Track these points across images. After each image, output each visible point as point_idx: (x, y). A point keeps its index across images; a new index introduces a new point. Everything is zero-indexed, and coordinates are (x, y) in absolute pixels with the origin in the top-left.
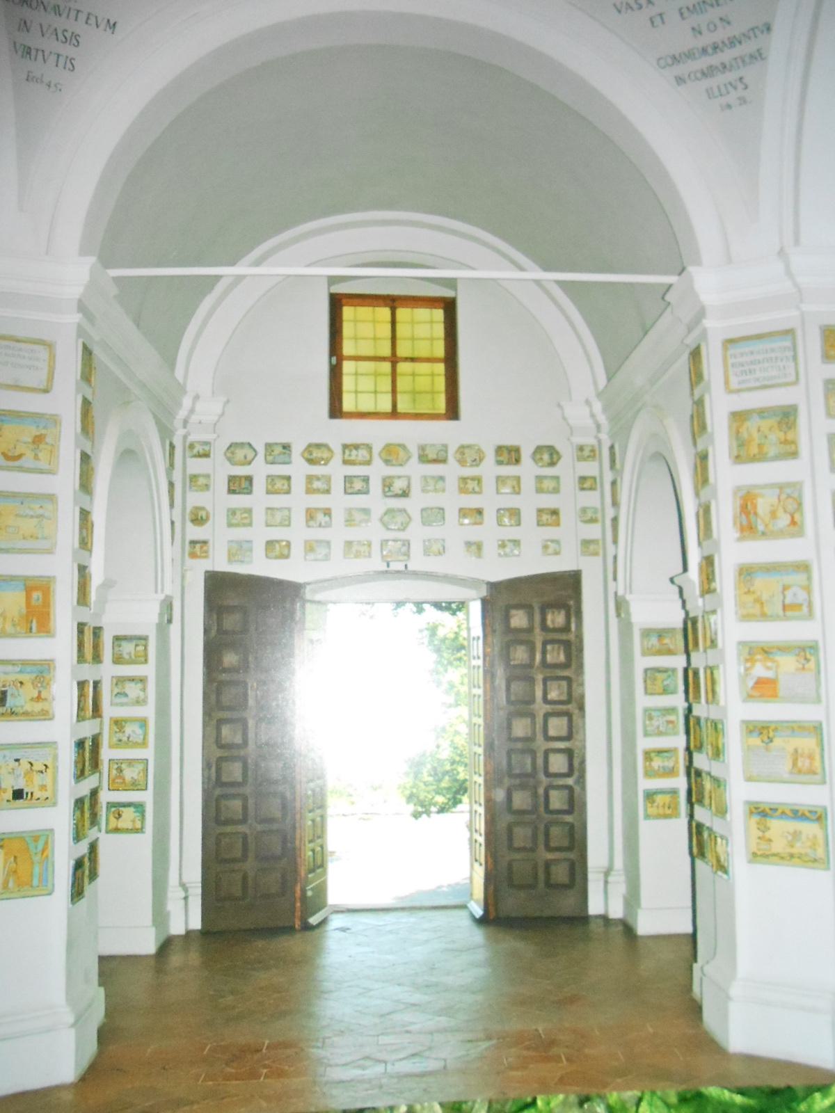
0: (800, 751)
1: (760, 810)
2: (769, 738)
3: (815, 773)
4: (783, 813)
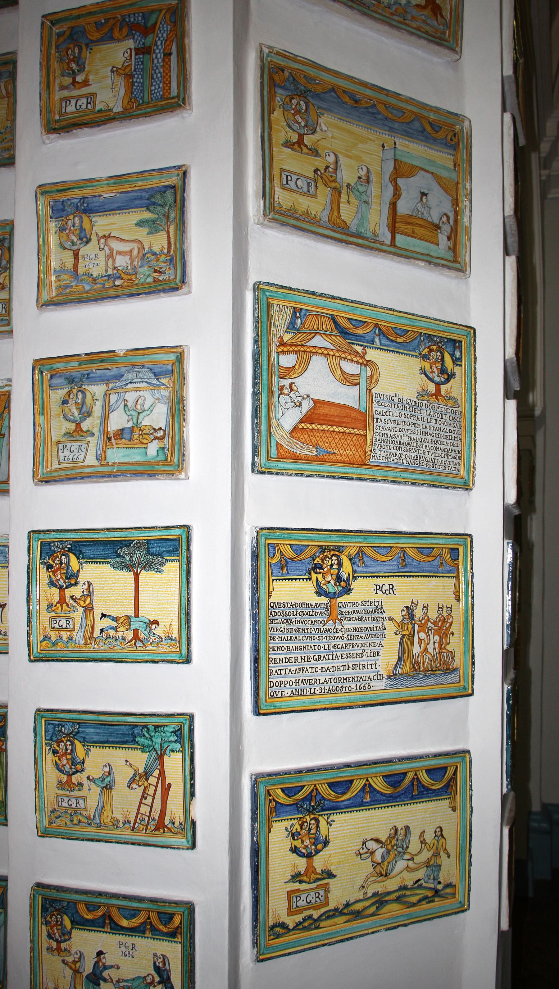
0: (419, 613)
1: (301, 795)
2: (339, 579)
3: (449, 670)
4: (368, 788)
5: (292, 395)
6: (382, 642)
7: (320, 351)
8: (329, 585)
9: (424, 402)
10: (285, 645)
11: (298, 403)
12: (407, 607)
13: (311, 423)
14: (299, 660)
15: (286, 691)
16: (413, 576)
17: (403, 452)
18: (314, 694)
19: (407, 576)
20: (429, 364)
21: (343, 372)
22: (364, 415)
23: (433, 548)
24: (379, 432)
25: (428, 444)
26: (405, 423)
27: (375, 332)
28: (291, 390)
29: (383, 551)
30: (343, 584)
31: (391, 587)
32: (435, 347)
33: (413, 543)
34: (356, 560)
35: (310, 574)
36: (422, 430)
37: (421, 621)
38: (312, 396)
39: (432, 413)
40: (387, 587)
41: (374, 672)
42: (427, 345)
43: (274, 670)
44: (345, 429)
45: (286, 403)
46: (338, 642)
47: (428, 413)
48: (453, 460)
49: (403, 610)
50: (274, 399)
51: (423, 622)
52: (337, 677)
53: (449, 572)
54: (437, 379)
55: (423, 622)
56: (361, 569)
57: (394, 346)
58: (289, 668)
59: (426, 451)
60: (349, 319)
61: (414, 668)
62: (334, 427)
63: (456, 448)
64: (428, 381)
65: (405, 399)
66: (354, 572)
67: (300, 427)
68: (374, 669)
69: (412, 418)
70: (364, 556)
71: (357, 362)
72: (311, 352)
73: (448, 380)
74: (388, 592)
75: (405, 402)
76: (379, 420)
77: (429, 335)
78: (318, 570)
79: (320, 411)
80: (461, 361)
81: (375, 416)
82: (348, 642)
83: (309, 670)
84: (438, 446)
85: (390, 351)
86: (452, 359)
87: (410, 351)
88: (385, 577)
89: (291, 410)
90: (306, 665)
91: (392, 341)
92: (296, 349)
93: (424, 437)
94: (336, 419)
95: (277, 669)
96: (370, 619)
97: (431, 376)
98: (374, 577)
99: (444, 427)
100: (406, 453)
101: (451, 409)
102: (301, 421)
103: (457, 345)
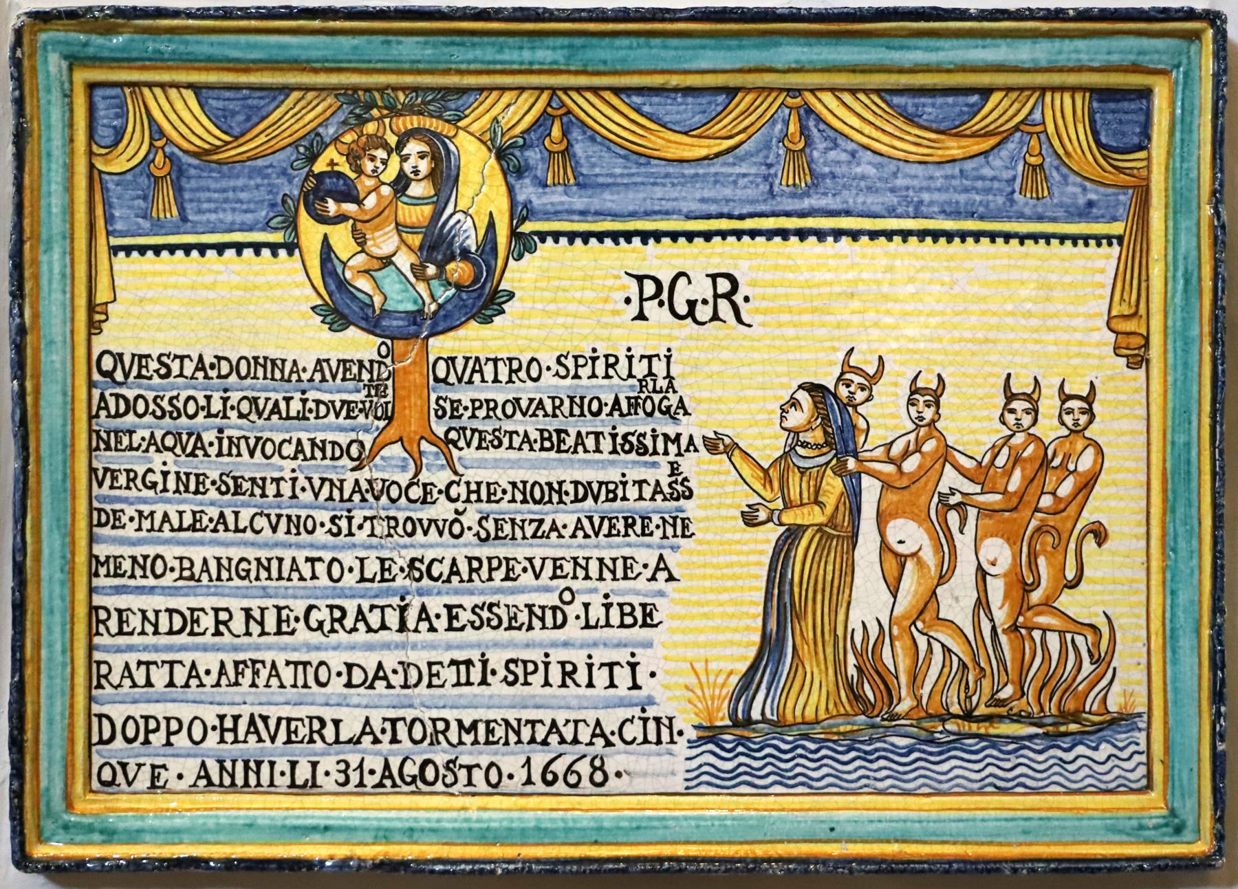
6: (671, 559)
8: (388, 279)
10: (170, 553)
12: (813, 389)
14: (238, 625)
15: (175, 766)
16: (855, 235)
18: (311, 785)
19: (820, 235)
23: (986, 92)
29: (685, 111)
30: (459, 270)
31: (724, 286)
33: (854, 69)
34: (533, 156)
35: (292, 224)
37: (897, 462)
40: (702, 289)
41: (622, 703)
43: (117, 661)
46: (432, 547)
49: (794, 403)
51: (910, 465)
52: (426, 715)
53: (1086, 212)
55: (910, 465)
56: (556, 197)
58: (187, 658)
61: (856, 697)
66: (520, 212)
68: (623, 690)
70: (576, 134)
74: (703, 313)
78: (332, 207)
82: (484, 552)
83: (287, 674)
88: (690, 236)
90: (274, 652)
95: (132, 658)
96: (606, 444)
98: (628, 236)
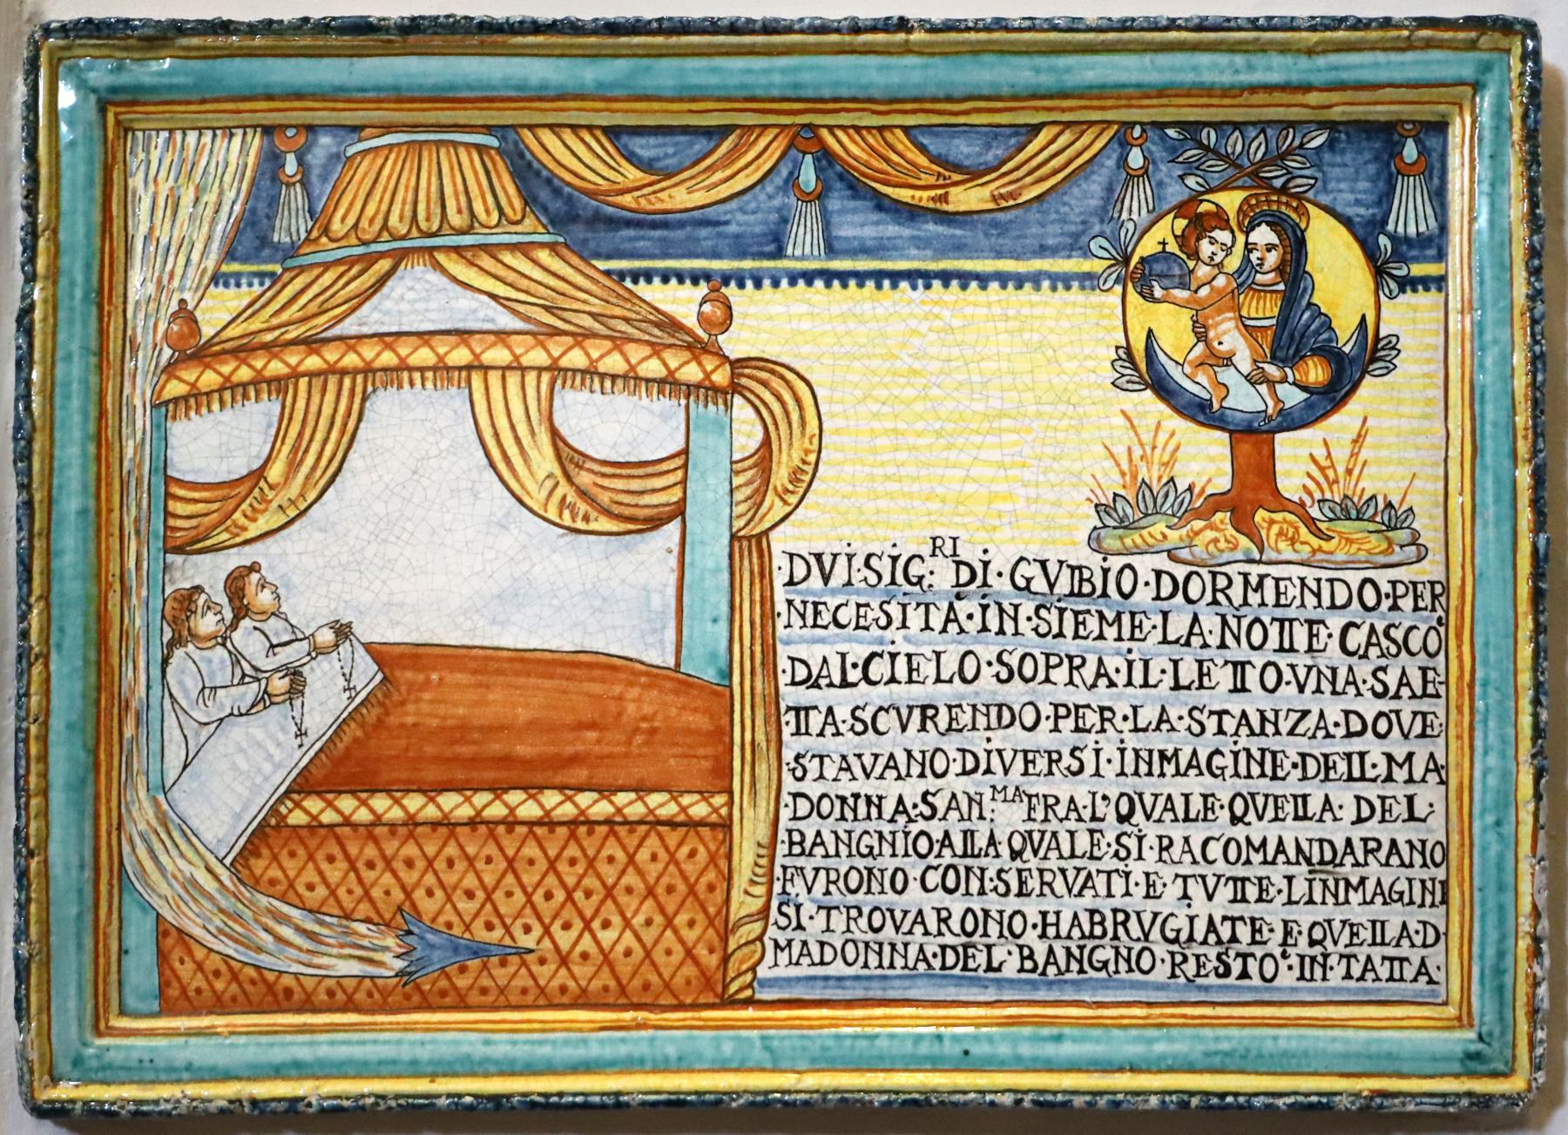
5: (247, 639)
7: (424, 356)
9: (1145, 566)
11: (280, 684)
13: (364, 784)
17: (993, 902)
20: (1185, 316)
21: (568, 457)
22: (719, 696)
24: (814, 790)
25: (1177, 832)
26: (1005, 716)
27: (792, 181)
28: (241, 611)
32: (1230, 201)
36: (1132, 741)
38: (372, 630)
39: (1210, 622)
42: (1175, 194)
44: (584, 799)
45: (208, 690)
47: (1179, 626)
48: (1378, 910)
50: (136, 679)
54: (1245, 400)
57: (922, 243)
59: (1167, 872)
60: (613, 132)
62: (514, 797)
63: (1403, 833)
64: (1175, 422)
65: (1000, 563)
67: (297, 818)
69: (1060, 675)
71: (669, 384)
72: (368, 370)
73: (1331, 397)
75: (1001, 585)
76: (816, 720)
77: (1191, 129)
79: (422, 711)
80: (1441, 256)
81: (792, 696)
84: (1257, 830)
85: (895, 277)
86: (1370, 252)
87: (1043, 251)
89: (237, 732)
91: (912, 213)
92: (276, 368)
93: (1148, 786)
94: (522, 750)
97: (1198, 385)
99: (1308, 701)
100: (1012, 903)
101: (1354, 578)
102: (303, 785)
103: (1410, 151)
